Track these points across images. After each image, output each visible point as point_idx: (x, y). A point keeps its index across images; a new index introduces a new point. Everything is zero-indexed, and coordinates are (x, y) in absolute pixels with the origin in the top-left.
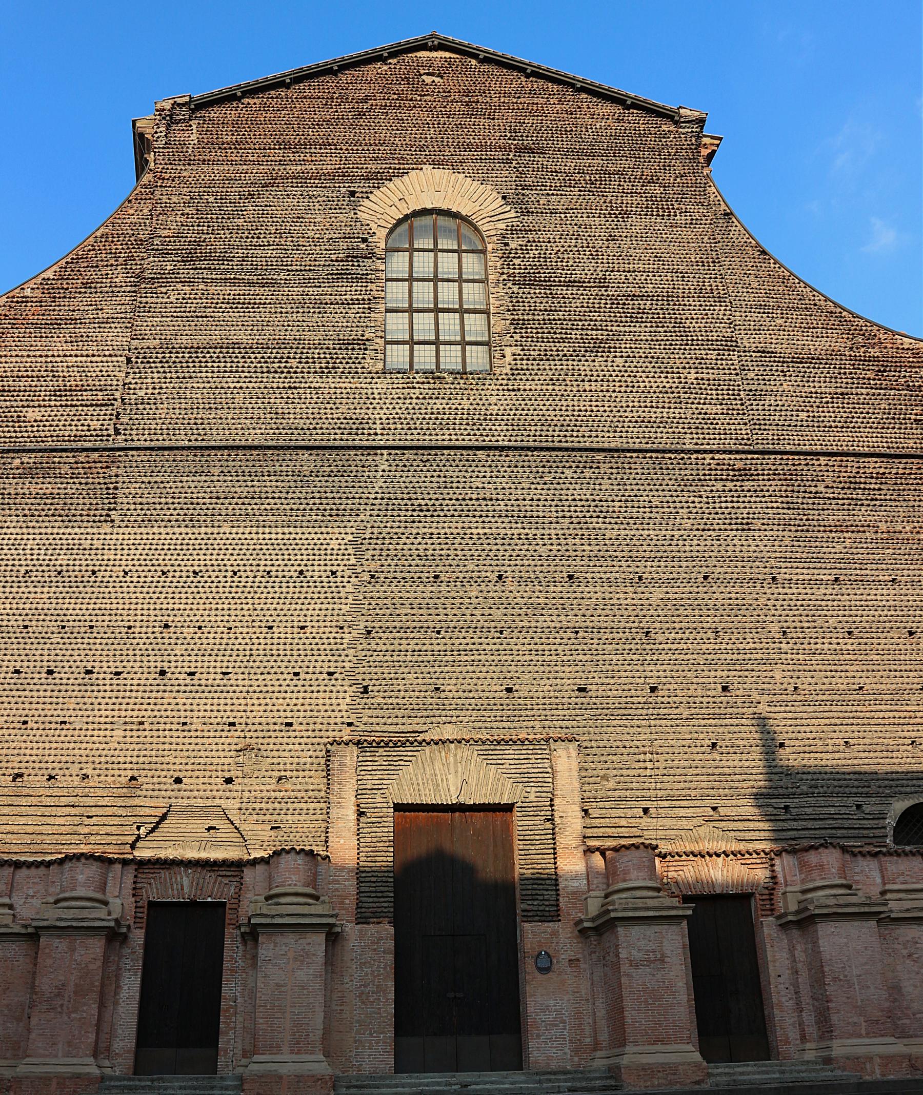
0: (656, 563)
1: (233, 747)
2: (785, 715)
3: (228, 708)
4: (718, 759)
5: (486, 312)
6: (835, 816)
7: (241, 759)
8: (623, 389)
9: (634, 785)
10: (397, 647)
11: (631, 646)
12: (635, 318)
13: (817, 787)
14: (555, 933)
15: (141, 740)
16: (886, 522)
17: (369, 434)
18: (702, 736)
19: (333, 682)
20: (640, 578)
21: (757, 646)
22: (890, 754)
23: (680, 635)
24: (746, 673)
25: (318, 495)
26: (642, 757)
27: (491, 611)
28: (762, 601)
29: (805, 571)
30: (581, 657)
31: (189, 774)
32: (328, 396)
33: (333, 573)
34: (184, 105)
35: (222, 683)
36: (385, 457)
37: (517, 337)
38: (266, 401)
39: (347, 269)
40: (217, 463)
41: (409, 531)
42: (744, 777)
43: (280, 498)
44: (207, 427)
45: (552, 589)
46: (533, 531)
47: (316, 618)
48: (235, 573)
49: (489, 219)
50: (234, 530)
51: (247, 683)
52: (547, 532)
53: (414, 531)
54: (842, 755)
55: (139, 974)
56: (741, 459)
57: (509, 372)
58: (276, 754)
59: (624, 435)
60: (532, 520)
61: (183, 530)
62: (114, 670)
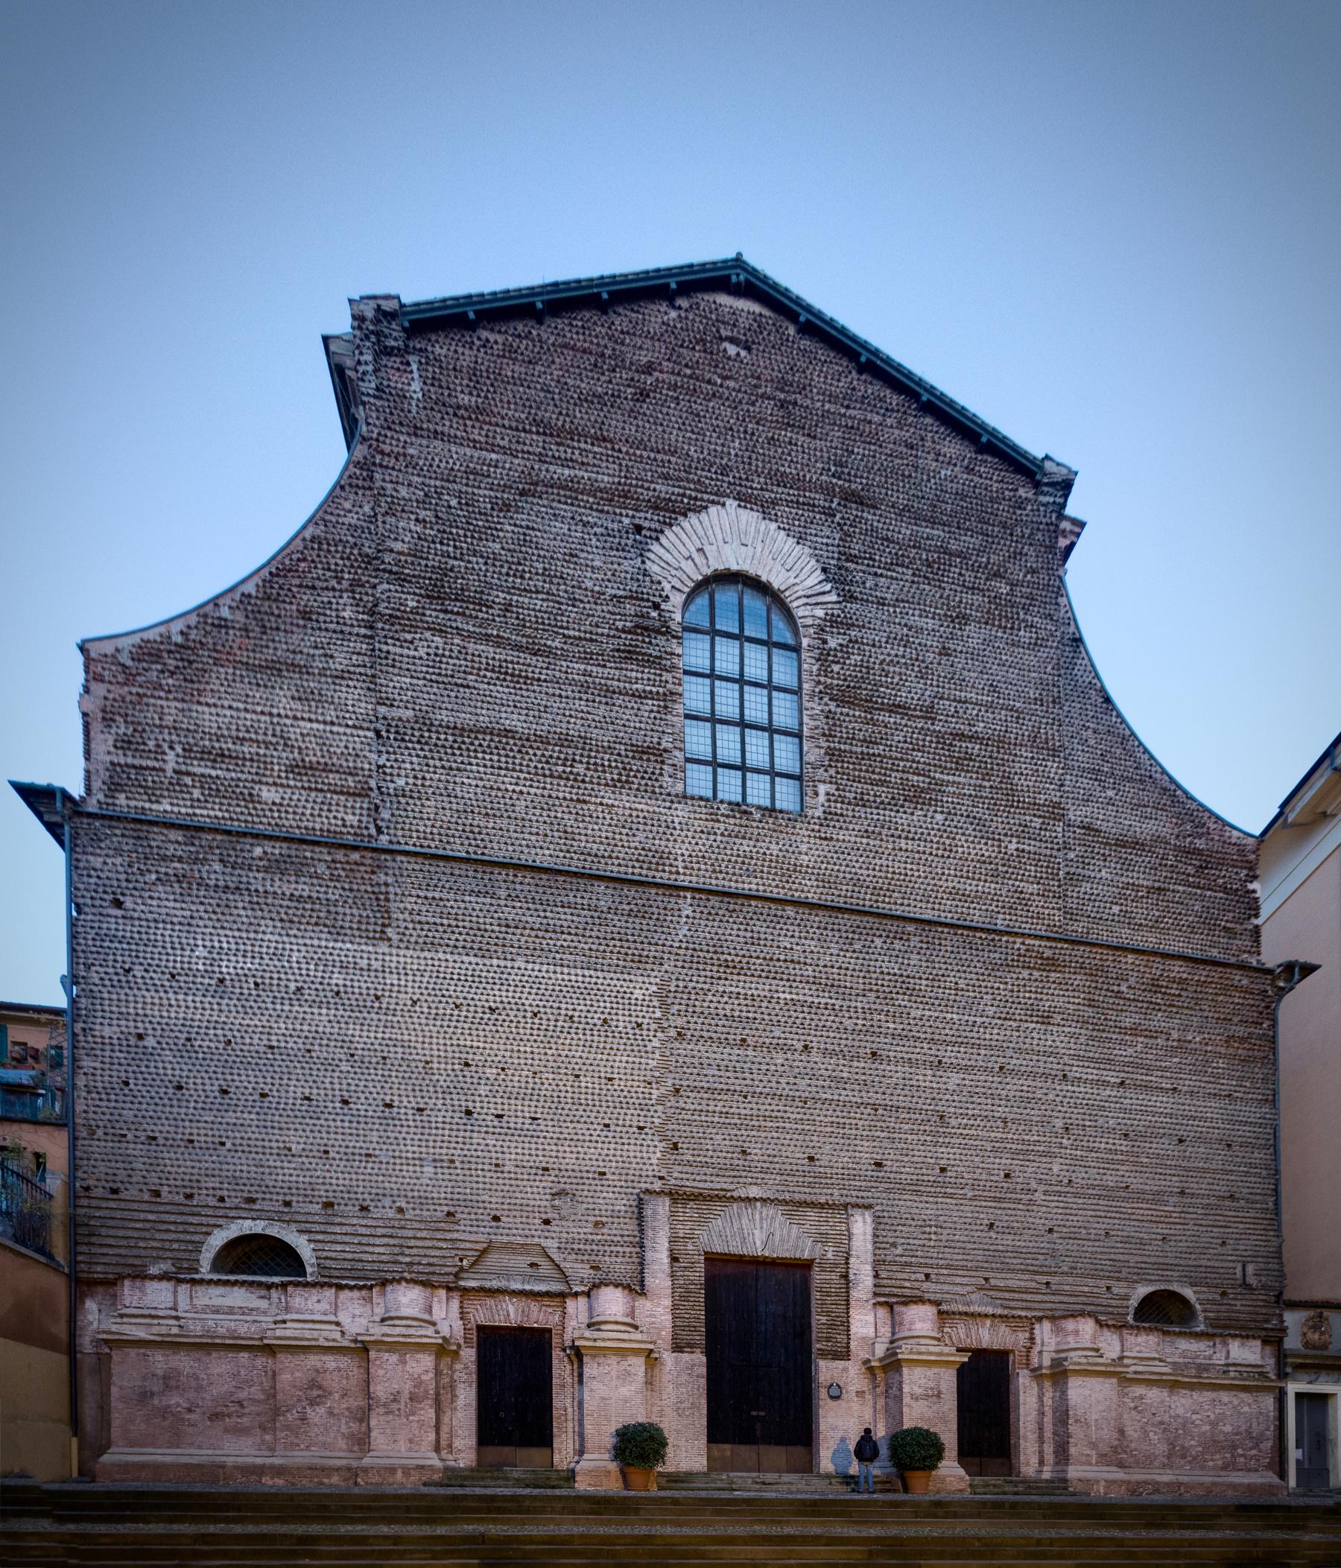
0: (956, 1049)
1: (548, 1191)
3: (540, 1153)
5: (799, 736)
7: (556, 1203)
8: (940, 853)
9: (919, 1253)
10: (705, 1108)
12: (961, 764)
14: (845, 1370)
15: (454, 1177)
17: (671, 872)
20: (940, 1062)
21: (1042, 1139)
25: (617, 936)
26: (928, 1229)
28: (1051, 1097)
31: (506, 1213)
32: (622, 819)
33: (639, 1025)
35: (531, 1128)
36: (689, 901)
37: (832, 772)
38: (552, 814)
39: (637, 646)
40: (503, 885)
41: (714, 988)
43: (576, 935)
44: (487, 838)
45: (855, 1064)
46: (840, 1002)
47: (623, 1071)
48: (535, 1015)
49: (804, 600)
50: (530, 966)
51: (557, 1130)
52: (853, 1004)
53: (721, 989)
55: (474, 1385)
57: (822, 816)
58: (591, 1200)
59: (937, 906)
60: (841, 990)
61: (473, 960)
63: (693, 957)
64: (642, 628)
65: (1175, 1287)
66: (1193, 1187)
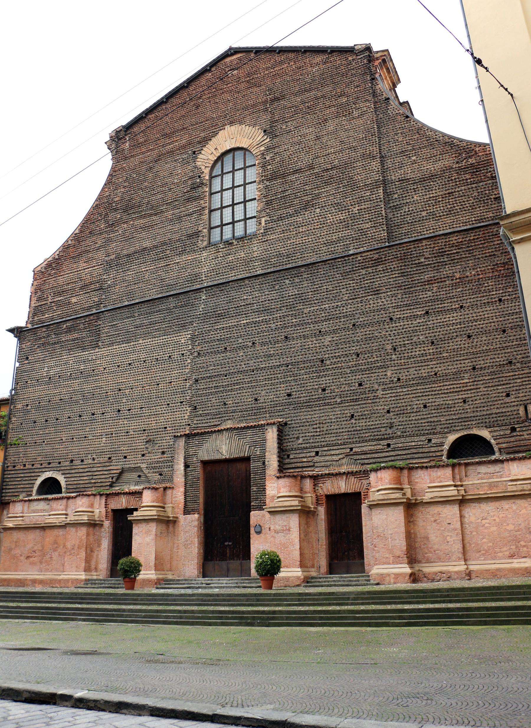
2: (391, 395)
4: (354, 422)
11: (314, 369)
13: (405, 432)
16: (460, 272)
18: (346, 412)
19: (182, 406)
20: (320, 332)
21: (379, 359)
22: (449, 410)
23: (338, 359)
24: (372, 375)
26: (315, 426)
27: (249, 362)
29: (408, 311)
30: (289, 379)
33: (183, 354)
34: (121, 130)
36: (205, 292)
42: (367, 431)
54: (422, 413)
56: (377, 253)
58: (160, 442)
62: (101, 412)
63: (206, 317)
64: (194, 188)
66: (480, 363)
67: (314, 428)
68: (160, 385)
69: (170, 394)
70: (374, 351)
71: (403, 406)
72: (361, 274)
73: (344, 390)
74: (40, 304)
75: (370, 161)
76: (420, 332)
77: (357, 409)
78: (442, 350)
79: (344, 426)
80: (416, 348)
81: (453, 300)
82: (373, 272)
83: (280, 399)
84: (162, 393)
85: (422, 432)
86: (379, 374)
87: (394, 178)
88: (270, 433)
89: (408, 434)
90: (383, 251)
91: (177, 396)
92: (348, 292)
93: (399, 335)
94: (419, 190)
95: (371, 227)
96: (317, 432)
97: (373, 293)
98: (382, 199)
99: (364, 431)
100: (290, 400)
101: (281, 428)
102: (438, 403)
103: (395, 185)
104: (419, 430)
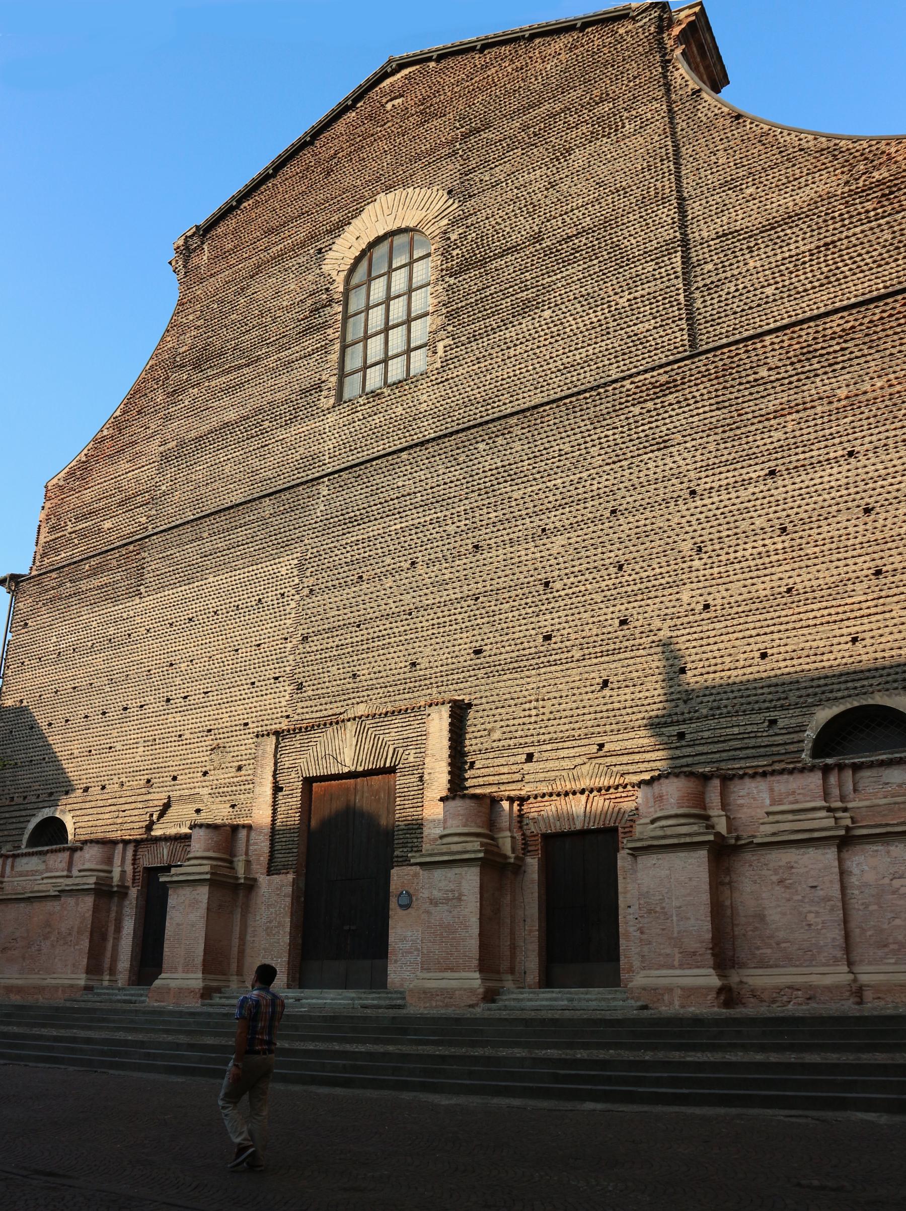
4: (608, 695)
6: (739, 737)
13: (719, 708)
18: (593, 675)
26: (527, 706)
42: (635, 709)
65: (879, 699)
67: (524, 710)
68: (240, 651)
69: (257, 666)
70: (653, 556)
71: (715, 658)
72: (631, 415)
73: (589, 634)
74: (53, 537)
75: (655, 209)
76: (756, 511)
77: (613, 669)
78: (804, 541)
79: (586, 703)
80: (745, 543)
81: (830, 443)
82: (655, 409)
83: (461, 659)
84: (243, 664)
85: (756, 706)
86: (664, 599)
87: (705, 235)
88: (436, 721)
89: (725, 710)
90: (679, 368)
91: (268, 668)
92: (603, 452)
93: (708, 522)
94: (759, 249)
95: (655, 328)
96: (530, 716)
97: (655, 447)
98: (680, 274)
99: (629, 711)
100: (479, 661)
101: (458, 711)
102: (794, 647)
103: (709, 246)
104: (749, 703)
